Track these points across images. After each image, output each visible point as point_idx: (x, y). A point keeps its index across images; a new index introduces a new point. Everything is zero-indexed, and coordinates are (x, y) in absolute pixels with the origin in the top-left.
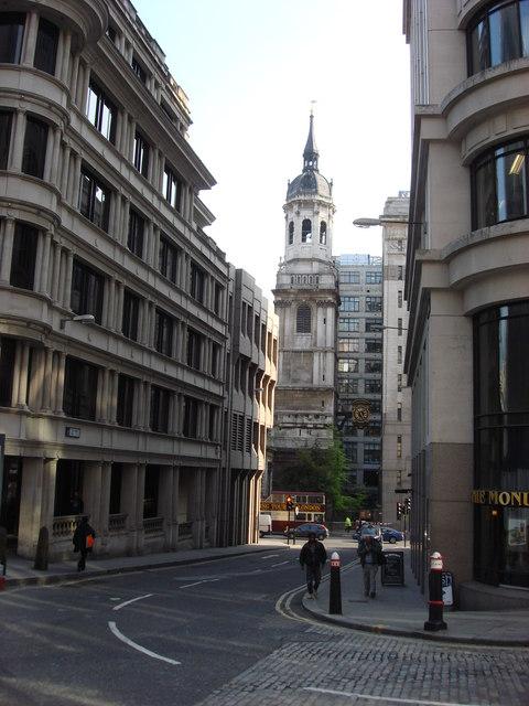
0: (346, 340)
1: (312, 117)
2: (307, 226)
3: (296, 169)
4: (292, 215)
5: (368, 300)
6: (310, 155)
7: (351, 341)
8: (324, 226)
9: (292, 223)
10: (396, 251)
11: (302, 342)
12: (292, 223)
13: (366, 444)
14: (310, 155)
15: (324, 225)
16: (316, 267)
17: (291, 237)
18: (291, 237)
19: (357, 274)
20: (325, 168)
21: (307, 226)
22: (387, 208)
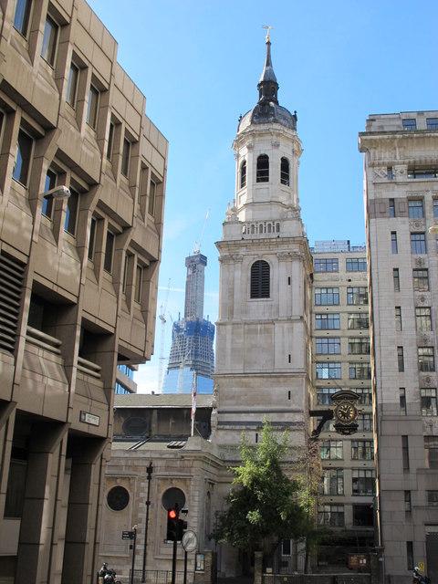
0: (326, 341)
1: (269, 43)
3: (254, 99)
4: (244, 151)
5: (350, 290)
6: (269, 88)
7: (331, 341)
8: (285, 165)
9: (244, 163)
10: (385, 180)
13: (353, 469)
14: (269, 88)
15: (285, 165)
16: (275, 213)
17: (243, 180)
18: (243, 180)
19: (335, 261)
20: (284, 98)
21: (263, 163)
22: (368, 126)
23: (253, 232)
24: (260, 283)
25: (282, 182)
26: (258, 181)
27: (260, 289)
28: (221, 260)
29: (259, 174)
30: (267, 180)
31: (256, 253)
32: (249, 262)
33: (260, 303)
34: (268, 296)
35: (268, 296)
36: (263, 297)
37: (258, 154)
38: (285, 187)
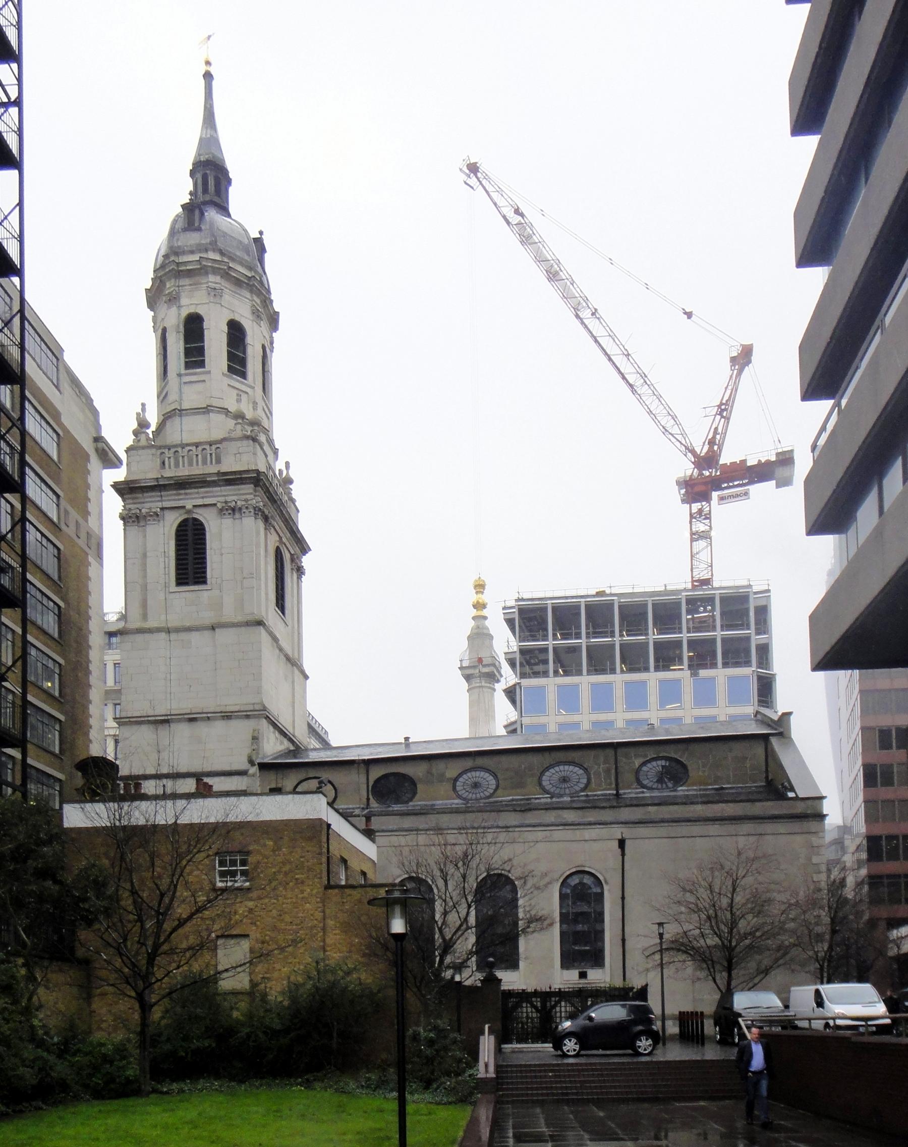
8: (236, 333)
9: (164, 330)
11: (187, 604)
12: (164, 330)
23: (177, 465)
24: (191, 563)
25: (230, 369)
26: (188, 365)
27: (190, 567)
28: (123, 518)
29: (188, 352)
30: (202, 364)
31: (181, 503)
32: (172, 521)
33: (189, 592)
34: (205, 582)
35: (205, 582)
36: (196, 583)
38: (236, 381)
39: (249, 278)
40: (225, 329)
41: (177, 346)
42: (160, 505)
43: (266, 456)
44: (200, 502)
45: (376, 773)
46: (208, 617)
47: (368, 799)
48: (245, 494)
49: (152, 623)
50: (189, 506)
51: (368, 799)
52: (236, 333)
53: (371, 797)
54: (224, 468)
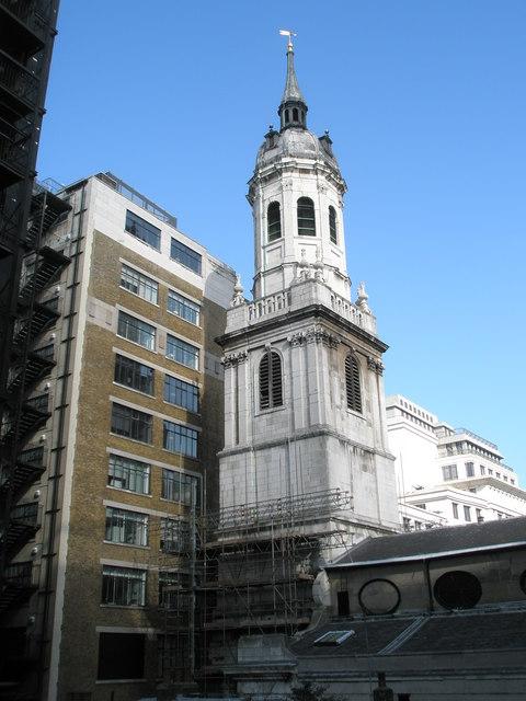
2: (274, 210)
30: (279, 235)
32: (257, 357)
37: (267, 204)
38: (307, 239)
39: (314, 166)
40: (296, 205)
41: (264, 224)
42: (247, 348)
43: (330, 289)
44: (275, 339)
45: (436, 573)
46: (283, 432)
47: (432, 602)
48: (312, 326)
49: (241, 445)
50: (268, 344)
51: (432, 602)
52: (306, 206)
53: (434, 599)
54: (294, 308)
